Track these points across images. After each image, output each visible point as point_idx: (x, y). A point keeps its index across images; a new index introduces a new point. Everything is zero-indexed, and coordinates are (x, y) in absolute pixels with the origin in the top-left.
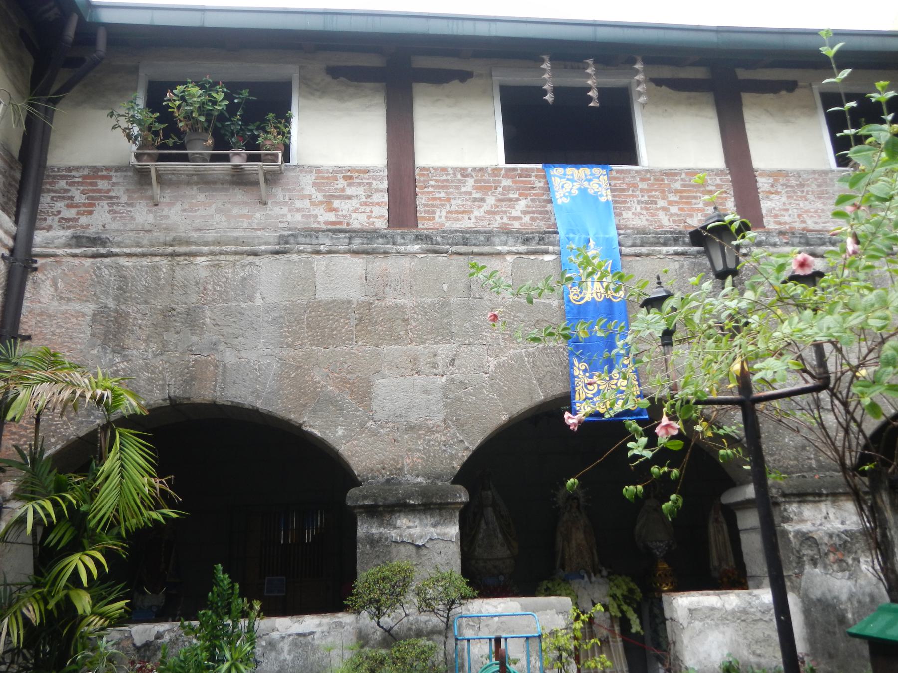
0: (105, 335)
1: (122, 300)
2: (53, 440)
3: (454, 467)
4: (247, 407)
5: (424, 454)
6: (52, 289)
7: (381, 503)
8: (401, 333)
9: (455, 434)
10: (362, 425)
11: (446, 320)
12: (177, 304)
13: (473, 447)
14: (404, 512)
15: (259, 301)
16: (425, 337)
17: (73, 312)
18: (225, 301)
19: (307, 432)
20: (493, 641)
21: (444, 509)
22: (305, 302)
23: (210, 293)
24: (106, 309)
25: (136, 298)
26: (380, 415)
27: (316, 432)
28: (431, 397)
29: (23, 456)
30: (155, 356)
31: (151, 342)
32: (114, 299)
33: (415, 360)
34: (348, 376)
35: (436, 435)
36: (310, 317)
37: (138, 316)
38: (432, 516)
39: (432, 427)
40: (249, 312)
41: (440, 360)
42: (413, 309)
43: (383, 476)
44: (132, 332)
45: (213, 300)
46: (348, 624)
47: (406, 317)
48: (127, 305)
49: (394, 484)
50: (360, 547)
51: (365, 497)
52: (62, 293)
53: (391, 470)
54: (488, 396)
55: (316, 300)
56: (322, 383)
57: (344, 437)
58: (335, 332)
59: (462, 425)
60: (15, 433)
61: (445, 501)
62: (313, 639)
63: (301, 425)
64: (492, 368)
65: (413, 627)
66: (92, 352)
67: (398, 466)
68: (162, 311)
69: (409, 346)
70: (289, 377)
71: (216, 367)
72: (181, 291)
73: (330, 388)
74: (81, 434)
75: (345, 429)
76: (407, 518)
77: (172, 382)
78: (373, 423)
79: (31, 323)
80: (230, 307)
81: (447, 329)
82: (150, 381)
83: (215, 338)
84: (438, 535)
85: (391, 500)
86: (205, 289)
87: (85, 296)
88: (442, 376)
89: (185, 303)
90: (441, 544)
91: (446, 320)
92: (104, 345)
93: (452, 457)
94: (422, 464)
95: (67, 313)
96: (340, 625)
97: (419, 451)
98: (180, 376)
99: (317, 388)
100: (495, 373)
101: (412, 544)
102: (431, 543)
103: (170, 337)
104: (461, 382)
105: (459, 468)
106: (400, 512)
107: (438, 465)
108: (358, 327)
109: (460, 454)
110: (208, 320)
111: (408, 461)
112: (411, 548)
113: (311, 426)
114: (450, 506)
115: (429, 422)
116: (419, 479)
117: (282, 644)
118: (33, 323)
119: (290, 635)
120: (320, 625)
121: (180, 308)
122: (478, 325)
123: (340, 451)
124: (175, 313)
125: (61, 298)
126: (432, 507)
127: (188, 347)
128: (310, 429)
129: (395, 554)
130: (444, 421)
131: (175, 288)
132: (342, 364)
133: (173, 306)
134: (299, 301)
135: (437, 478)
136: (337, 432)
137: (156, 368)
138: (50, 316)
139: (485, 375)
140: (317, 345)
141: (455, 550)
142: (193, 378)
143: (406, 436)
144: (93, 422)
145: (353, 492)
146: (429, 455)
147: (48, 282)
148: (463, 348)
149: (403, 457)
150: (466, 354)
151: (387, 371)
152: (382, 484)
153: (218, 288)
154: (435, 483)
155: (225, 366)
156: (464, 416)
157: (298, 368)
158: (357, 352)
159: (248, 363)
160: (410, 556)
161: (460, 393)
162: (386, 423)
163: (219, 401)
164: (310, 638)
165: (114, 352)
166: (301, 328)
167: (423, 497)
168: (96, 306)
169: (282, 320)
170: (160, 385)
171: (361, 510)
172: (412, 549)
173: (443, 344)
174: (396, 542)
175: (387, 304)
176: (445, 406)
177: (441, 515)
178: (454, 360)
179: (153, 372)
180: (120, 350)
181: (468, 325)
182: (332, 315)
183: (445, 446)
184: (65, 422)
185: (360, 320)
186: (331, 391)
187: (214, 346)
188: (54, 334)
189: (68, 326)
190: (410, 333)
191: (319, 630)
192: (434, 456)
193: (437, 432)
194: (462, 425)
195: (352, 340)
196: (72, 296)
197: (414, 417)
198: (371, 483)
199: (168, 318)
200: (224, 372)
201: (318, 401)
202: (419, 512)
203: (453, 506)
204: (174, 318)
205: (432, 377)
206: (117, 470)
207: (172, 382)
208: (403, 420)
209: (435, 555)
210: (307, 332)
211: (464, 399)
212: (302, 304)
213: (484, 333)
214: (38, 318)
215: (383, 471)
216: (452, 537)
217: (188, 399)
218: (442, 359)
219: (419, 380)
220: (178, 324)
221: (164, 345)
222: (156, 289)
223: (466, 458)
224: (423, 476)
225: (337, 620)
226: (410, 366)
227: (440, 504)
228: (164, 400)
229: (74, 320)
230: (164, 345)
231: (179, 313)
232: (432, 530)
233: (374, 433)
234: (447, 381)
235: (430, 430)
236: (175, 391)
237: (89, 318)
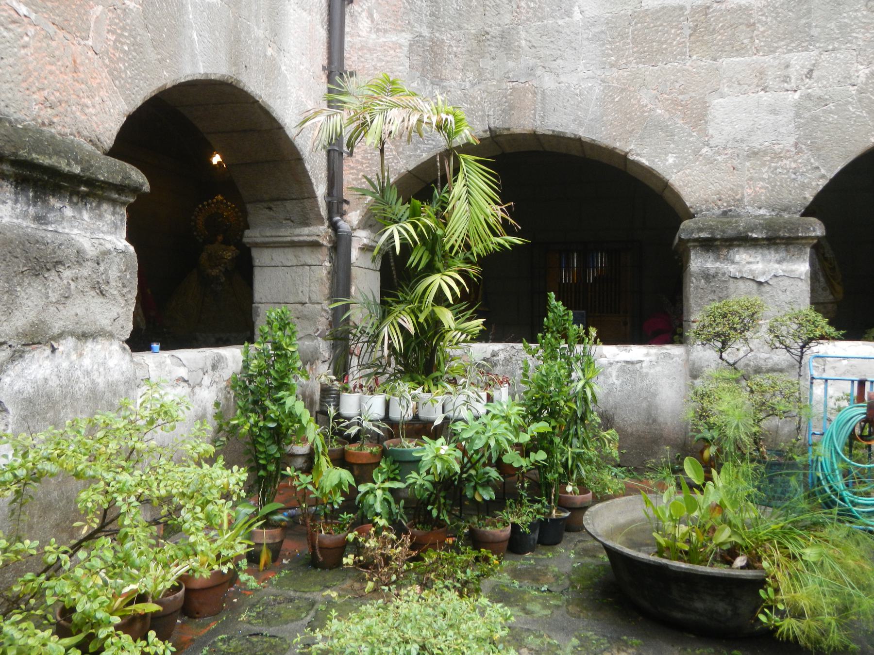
0: (423, 67)
1: (435, 27)
3: (805, 198)
4: (568, 135)
5: (769, 183)
6: (369, 22)
7: (719, 237)
8: (745, 41)
9: (808, 160)
10: (696, 152)
11: (803, 21)
12: (491, 26)
13: (831, 175)
14: (745, 247)
15: (577, 16)
16: (775, 45)
17: (391, 45)
18: (541, 19)
19: (633, 162)
20: (856, 383)
21: (791, 244)
22: (630, 13)
23: (524, 11)
24: (421, 39)
25: (449, 23)
26: (717, 140)
27: (645, 161)
28: (780, 117)
29: (374, 186)
30: (473, 85)
31: (467, 70)
32: (427, 27)
33: (762, 73)
34: (680, 97)
35: (785, 161)
36: (636, 30)
37: (453, 43)
38: (777, 251)
39: (780, 153)
40: (566, 30)
41: (793, 73)
42: (761, 10)
43: (719, 208)
44: (448, 61)
45: (528, 19)
46: (677, 356)
47: (752, 21)
48: (441, 33)
49: (732, 216)
50: (694, 281)
51: (701, 230)
52: (378, 24)
53: (728, 202)
54: (854, 113)
55: (643, 9)
56: (649, 106)
57: (675, 165)
58: (664, 46)
59: (818, 149)
60: (352, 168)
61: (795, 235)
62: (641, 367)
63: (627, 153)
64: (862, 79)
65: (752, 363)
66: (413, 85)
67: (737, 197)
68: (476, 36)
69: (754, 57)
70: (613, 101)
71: (535, 93)
72: (494, 12)
73: (659, 111)
74: (411, 168)
75: (676, 157)
76: (748, 253)
77: (491, 113)
78: (709, 150)
79: (353, 59)
80: (546, 26)
81: (806, 32)
83: (532, 62)
84: (784, 271)
85: (730, 233)
86: (518, 7)
87: (400, 25)
88: (795, 91)
89: (499, 25)
90: (787, 282)
91: (803, 21)
92: (423, 76)
93: (804, 186)
94: (765, 195)
95: (385, 45)
96: (669, 356)
97: (763, 180)
98: (499, 105)
99: (645, 112)
100: (866, 84)
101: (753, 280)
102: (775, 280)
103: (487, 64)
104: (820, 98)
105: (811, 199)
106: (739, 246)
107: (785, 195)
108: (692, 38)
109: (814, 184)
110: (523, 42)
111: (750, 191)
112: (752, 284)
113: (638, 155)
114: (799, 241)
115: (776, 147)
116: (762, 212)
117: (610, 369)
118: (355, 58)
119: (617, 362)
120: (647, 355)
121: (494, 31)
122: (846, 25)
123: (671, 181)
124: (489, 37)
125: (378, 30)
126: (778, 241)
127: (505, 73)
128: (637, 158)
129: (733, 290)
130: (796, 145)
131: (488, 8)
132: (672, 83)
134: (623, 12)
135: (784, 210)
136: (667, 160)
137: (475, 98)
138: (369, 50)
139: (851, 88)
140: (644, 63)
141: (804, 288)
142: (511, 107)
143: (748, 164)
144: (420, 156)
145: (686, 224)
146: (776, 185)
147: (364, 14)
148: (825, 56)
149: (742, 187)
150: (828, 62)
151: (726, 89)
152: (718, 217)
153: (532, 5)
154: (781, 216)
155: (543, 91)
156: (821, 138)
157: (623, 90)
158: (690, 68)
159: (568, 87)
160: (750, 293)
161: (818, 111)
162: (725, 149)
163: (540, 131)
164: (638, 366)
166: (625, 44)
167: (769, 230)
168: (412, 36)
169: (603, 36)
170: (480, 116)
171: (696, 244)
172: (754, 286)
173: (799, 51)
174: (736, 278)
175: (729, 7)
176: (798, 127)
177: (787, 251)
178: (811, 71)
179: (472, 103)
181: (832, 25)
182: (661, 25)
183: (795, 174)
184: (394, 156)
185: (695, 29)
186: (660, 115)
187: (531, 71)
188: (376, 69)
189: (388, 58)
190: (757, 41)
191: (647, 359)
192: (782, 185)
193: (786, 158)
194: (818, 149)
195: (684, 54)
196: (388, 27)
197: (759, 142)
198: (705, 216)
199: (482, 44)
200: (543, 98)
201: (646, 127)
202: (762, 246)
203: (804, 241)
204: (488, 42)
205: (781, 93)
206: (464, 196)
207: (491, 113)
208: (744, 145)
209: (780, 292)
210: (633, 48)
211: (823, 119)
212: (627, 15)
213: (854, 35)
214: (360, 53)
215: (719, 203)
216: (801, 274)
217: (508, 129)
218: (796, 70)
219: (766, 98)
220: (493, 49)
221: (480, 72)
222: (469, 13)
223: (821, 188)
224: (766, 208)
225: (665, 351)
226: (756, 81)
227: (789, 238)
228: (485, 131)
229: (392, 52)
230: (480, 72)
231: (493, 37)
232: (777, 266)
233: (710, 161)
234: (801, 97)
235: (777, 156)
236: (496, 122)
237: (406, 49)
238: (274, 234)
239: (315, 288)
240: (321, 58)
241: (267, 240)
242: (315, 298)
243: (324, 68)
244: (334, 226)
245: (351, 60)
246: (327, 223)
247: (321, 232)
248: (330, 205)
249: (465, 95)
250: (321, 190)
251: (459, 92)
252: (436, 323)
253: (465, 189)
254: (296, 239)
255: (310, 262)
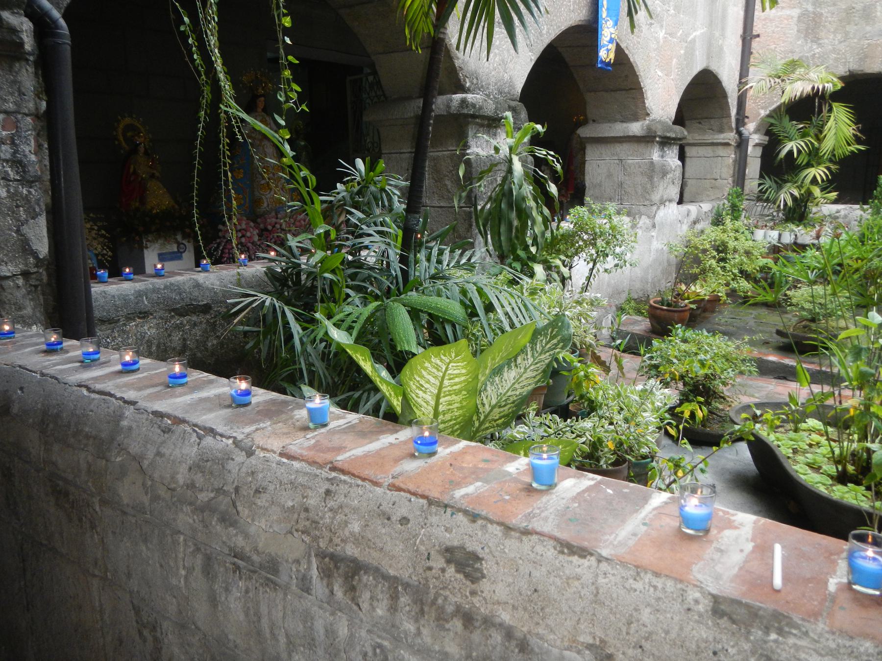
2: (775, 99)
12: (856, 3)
32: (812, 5)
37: (829, 15)
44: (824, 26)
66: (798, 43)
77: (851, 60)
82: (836, 60)
92: (806, 36)
98: (857, 55)
103: (851, 28)
118: (760, 26)
133: (854, 5)
138: (771, 20)
142: (866, 57)
165: (812, 41)
179: (838, 54)
180: (816, 40)
188: (774, 33)
206: (833, 126)
207: (851, 60)
221: (847, 34)
231: (858, 11)
237: (795, 19)
238: (701, 137)
239: (725, 170)
240: (740, 31)
241: (696, 141)
242: (724, 176)
243: (741, 36)
244: (740, 133)
245: (757, 28)
246: (735, 131)
247: (731, 136)
248: (737, 120)
249: (834, 48)
250: (733, 112)
251: (830, 47)
252: (809, 193)
253: (835, 122)
254: (715, 141)
255: (722, 155)
